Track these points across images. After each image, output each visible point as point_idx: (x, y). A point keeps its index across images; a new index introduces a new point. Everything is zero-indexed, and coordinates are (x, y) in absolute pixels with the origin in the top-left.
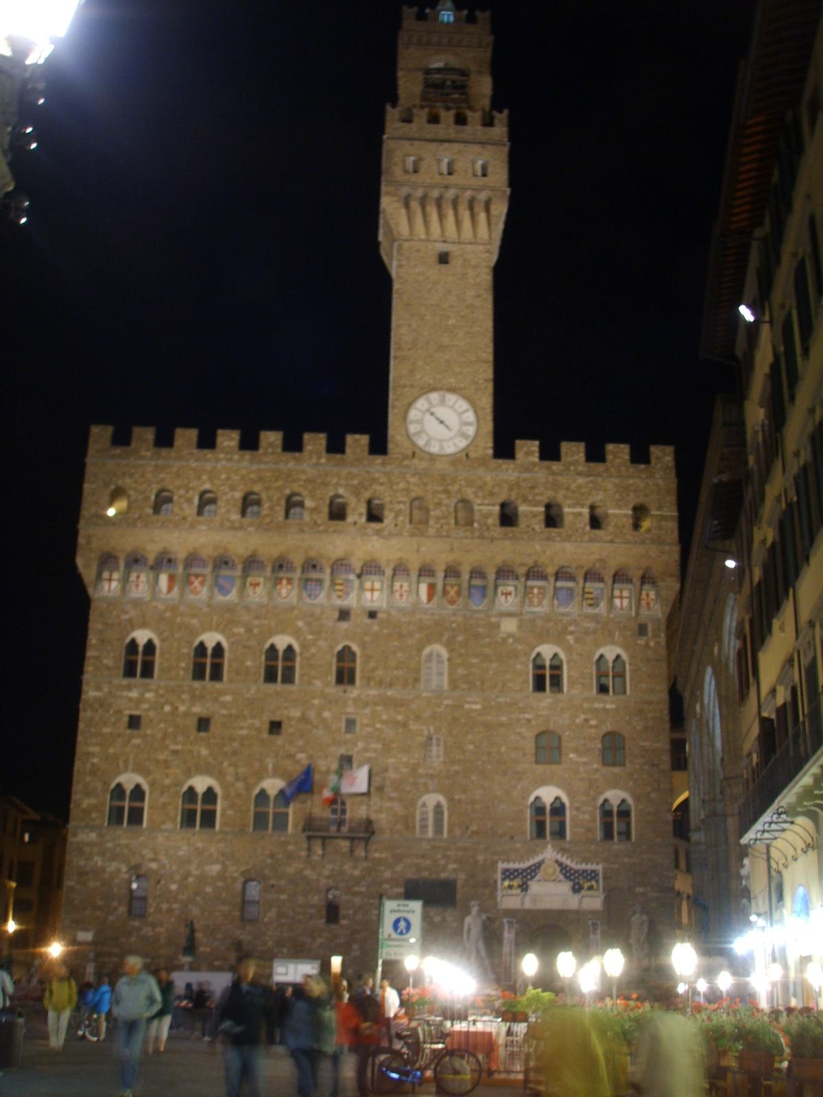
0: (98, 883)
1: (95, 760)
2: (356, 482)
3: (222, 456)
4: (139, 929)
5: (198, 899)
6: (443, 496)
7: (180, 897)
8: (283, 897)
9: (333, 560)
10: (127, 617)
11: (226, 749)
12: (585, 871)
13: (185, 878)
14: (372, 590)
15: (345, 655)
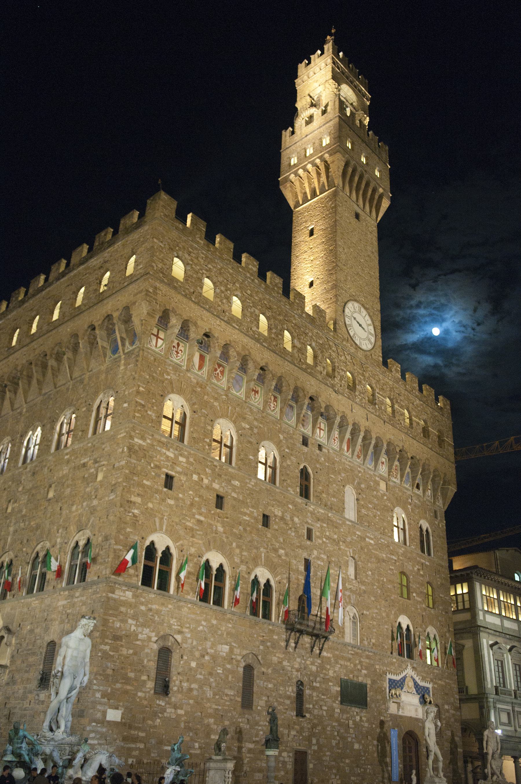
0: (131, 651)
1: (136, 511)
2: (321, 342)
3: (248, 275)
4: (163, 711)
5: (212, 680)
6: (362, 378)
7: (199, 676)
8: (270, 686)
9: (310, 395)
10: (169, 377)
11: (234, 530)
12: (424, 687)
13: (203, 656)
14: (320, 429)
15: (304, 474)
